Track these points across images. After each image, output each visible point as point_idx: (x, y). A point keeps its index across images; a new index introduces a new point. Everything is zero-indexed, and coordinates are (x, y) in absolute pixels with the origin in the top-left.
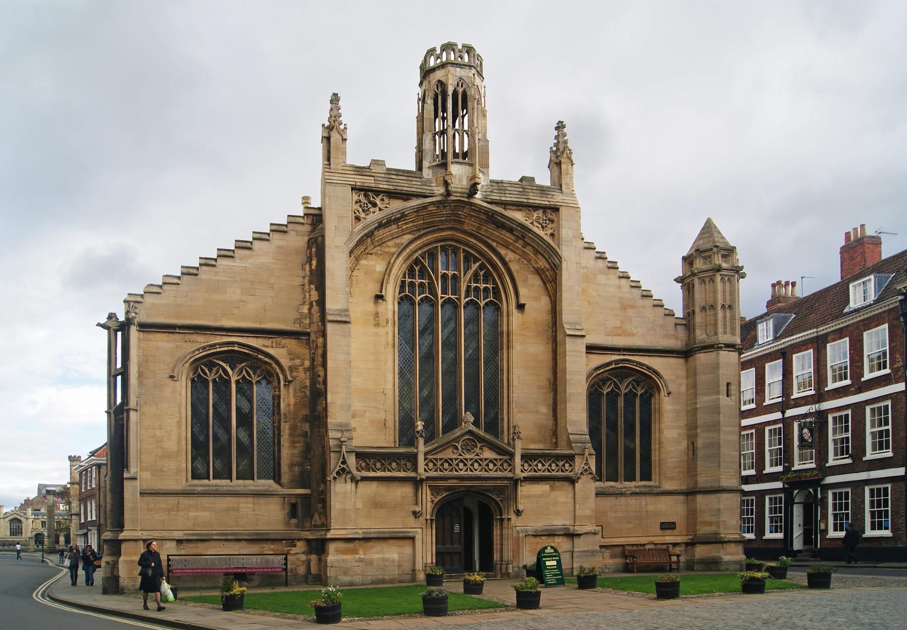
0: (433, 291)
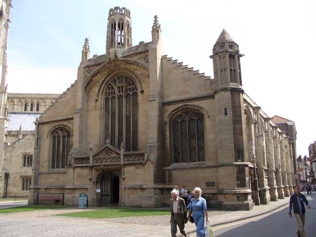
0: (115, 94)
